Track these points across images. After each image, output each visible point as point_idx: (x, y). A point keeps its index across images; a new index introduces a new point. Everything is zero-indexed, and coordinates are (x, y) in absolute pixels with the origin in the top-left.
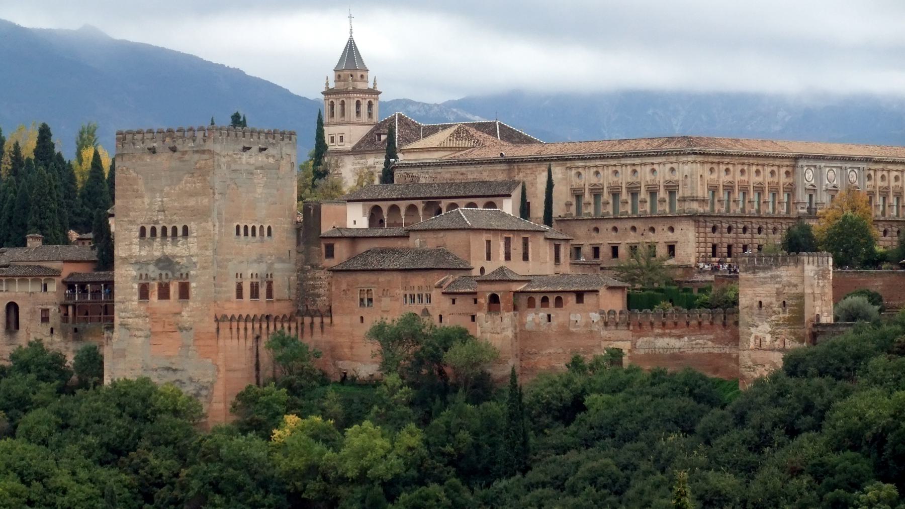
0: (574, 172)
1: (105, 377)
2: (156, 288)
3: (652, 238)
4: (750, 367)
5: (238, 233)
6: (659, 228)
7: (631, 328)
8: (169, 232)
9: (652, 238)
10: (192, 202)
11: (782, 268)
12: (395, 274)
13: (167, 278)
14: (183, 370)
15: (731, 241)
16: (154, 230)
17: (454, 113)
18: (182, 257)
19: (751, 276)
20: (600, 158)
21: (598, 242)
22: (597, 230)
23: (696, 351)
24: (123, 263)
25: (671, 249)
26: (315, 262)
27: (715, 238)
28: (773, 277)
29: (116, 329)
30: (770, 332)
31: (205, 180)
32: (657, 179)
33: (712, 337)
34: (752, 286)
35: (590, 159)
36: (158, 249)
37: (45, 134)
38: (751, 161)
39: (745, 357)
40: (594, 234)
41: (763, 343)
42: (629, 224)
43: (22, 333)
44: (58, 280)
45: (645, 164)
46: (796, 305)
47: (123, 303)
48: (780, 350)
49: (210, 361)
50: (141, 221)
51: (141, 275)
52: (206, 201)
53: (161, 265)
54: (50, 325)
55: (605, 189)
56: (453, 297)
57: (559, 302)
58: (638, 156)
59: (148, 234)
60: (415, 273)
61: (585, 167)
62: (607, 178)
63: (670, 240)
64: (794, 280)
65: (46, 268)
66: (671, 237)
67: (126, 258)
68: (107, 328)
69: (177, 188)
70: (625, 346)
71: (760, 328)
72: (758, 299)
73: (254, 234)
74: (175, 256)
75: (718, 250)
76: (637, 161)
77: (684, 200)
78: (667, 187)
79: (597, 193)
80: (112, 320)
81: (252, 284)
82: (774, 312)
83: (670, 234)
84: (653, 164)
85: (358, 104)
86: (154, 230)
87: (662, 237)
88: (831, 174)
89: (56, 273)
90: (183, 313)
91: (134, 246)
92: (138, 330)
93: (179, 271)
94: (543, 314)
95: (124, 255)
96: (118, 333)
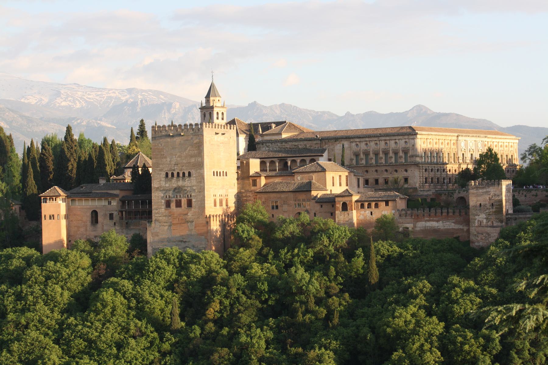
0: (354, 144)
1: (148, 246)
2: (175, 202)
3: (396, 175)
4: (475, 235)
5: (214, 175)
6: (399, 170)
7: (413, 217)
8: (181, 175)
9: (396, 175)
10: (193, 160)
11: (491, 188)
12: (289, 193)
13: (180, 197)
14: (189, 242)
15: (427, 176)
16: (173, 174)
17: (99, 123)
18: (188, 187)
19: (475, 192)
20: (368, 137)
21: (367, 177)
22: (367, 171)
23: (445, 227)
24: (157, 190)
25: (406, 180)
26: (247, 188)
27: (426, 175)
28: (487, 192)
29: (153, 222)
30: (485, 218)
31: (199, 149)
32: (398, 146)
33: (454, 221)
34: (476, 197)
35: (363, 137)
36: (175, 183)
37: (69, 129)
38: (422, 137)
39: (473, 230)
40: (366, 173)
41: (482, 223)
42: (384, 168)
43: (99, 225)
44: (117, 199)
45: (391, 140)
46: (498, 205)
47: (157, 209)
48: (490, 227)
49: (203, 237)
50: (166, 169)
51: (166, 196)
52: (200, 159)
53: (177, 191)
54: (114, 221)
55: (371, 152)
56: (321, 204)
57: (377, 206)
58: (388, 136)
59: (170, 175)
60: (301, 193)
61: (360, 142)
62: (372, 146)
63: (405, 176)
64: (497, 193)
65: (111, 194)
66: (405, 174)
67: (158, 188)
68: (148, 222)
69: (184, 153)
70: (410, 226)
71: (480, 216)
72: (479, 203)
73: (220, 176)
74: (184, 186)
75: (428, 180)
76: (388, 138)
77: (412, 156)
78: (403, 151)
79: (367, 154)
80: (151, 218)
81: (220, 200)
82: (487, 208)
83: (405, 173)
84: (395, 139)
85: (218, 113)
86: (173, 174)
87: (401, 175)
88: (471, 144)
89: (117, 196)
90: (189, 214)
91: (162, 182)
92: (164, 222)
93: (186, 193)
94: (368, 212)
95: (157, 186)
96: (153, 224)
